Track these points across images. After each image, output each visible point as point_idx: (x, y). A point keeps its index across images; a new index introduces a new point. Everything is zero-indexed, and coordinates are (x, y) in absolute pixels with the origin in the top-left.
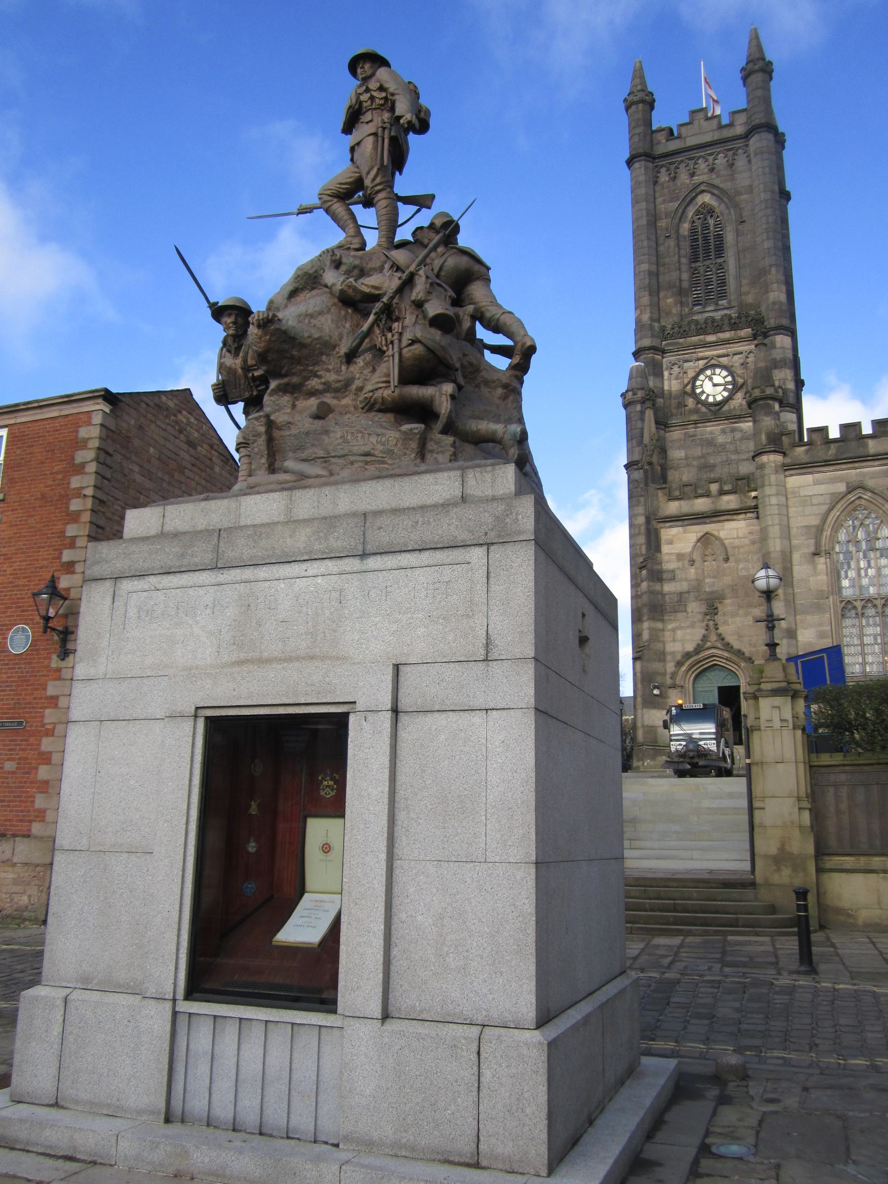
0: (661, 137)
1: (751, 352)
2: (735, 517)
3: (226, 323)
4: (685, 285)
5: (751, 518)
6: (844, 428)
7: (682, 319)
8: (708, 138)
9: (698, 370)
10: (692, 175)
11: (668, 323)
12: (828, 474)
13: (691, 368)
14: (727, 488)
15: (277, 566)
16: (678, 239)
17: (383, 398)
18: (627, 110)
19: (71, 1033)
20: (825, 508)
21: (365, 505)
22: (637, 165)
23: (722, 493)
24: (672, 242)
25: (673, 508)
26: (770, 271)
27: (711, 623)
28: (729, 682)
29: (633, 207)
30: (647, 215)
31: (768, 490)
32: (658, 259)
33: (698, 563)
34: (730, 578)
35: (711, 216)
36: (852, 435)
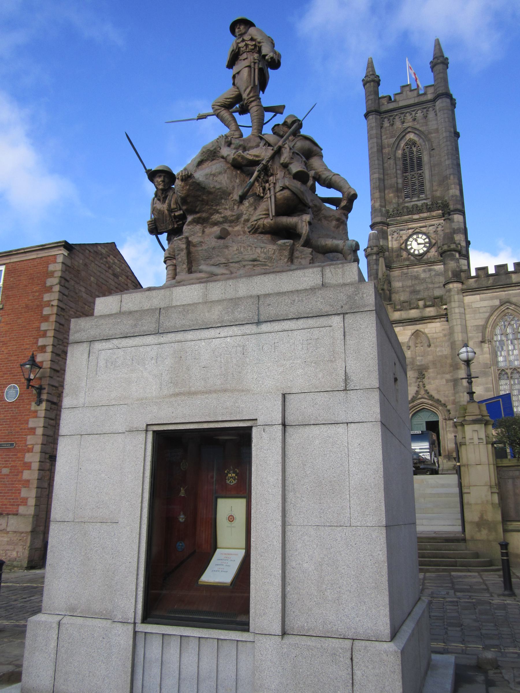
0: (384, 101)
1: (439, 224)
2: (433, 321)
3: (157, 181)
4: (400, 186)
5: (442, 321)
6: (497, 267)
7: (398, 206)
8: (411, 102)
9: (408, 235)
10: (403, 123)
11: (390, 208)
12: (489, 294)
13: (404, 234)
14: (428, 303)
15: (199, 331)
16: (395, 159)
17: (263, 224)
18: (364, 85)
19: (63, 646)
20: (488, 314)
22: (370, 117)
23: (426, 306)
24: (392, 162)
26: (450, 177)
27: (421, 383)
28: (432, 419)
29: (369, 141)
30: (377, 146)
31: (453, 305)
32: (384, 171)
33: (412, 348)
34: (432, 356)
35: (415, 146)
36: (503, 272)
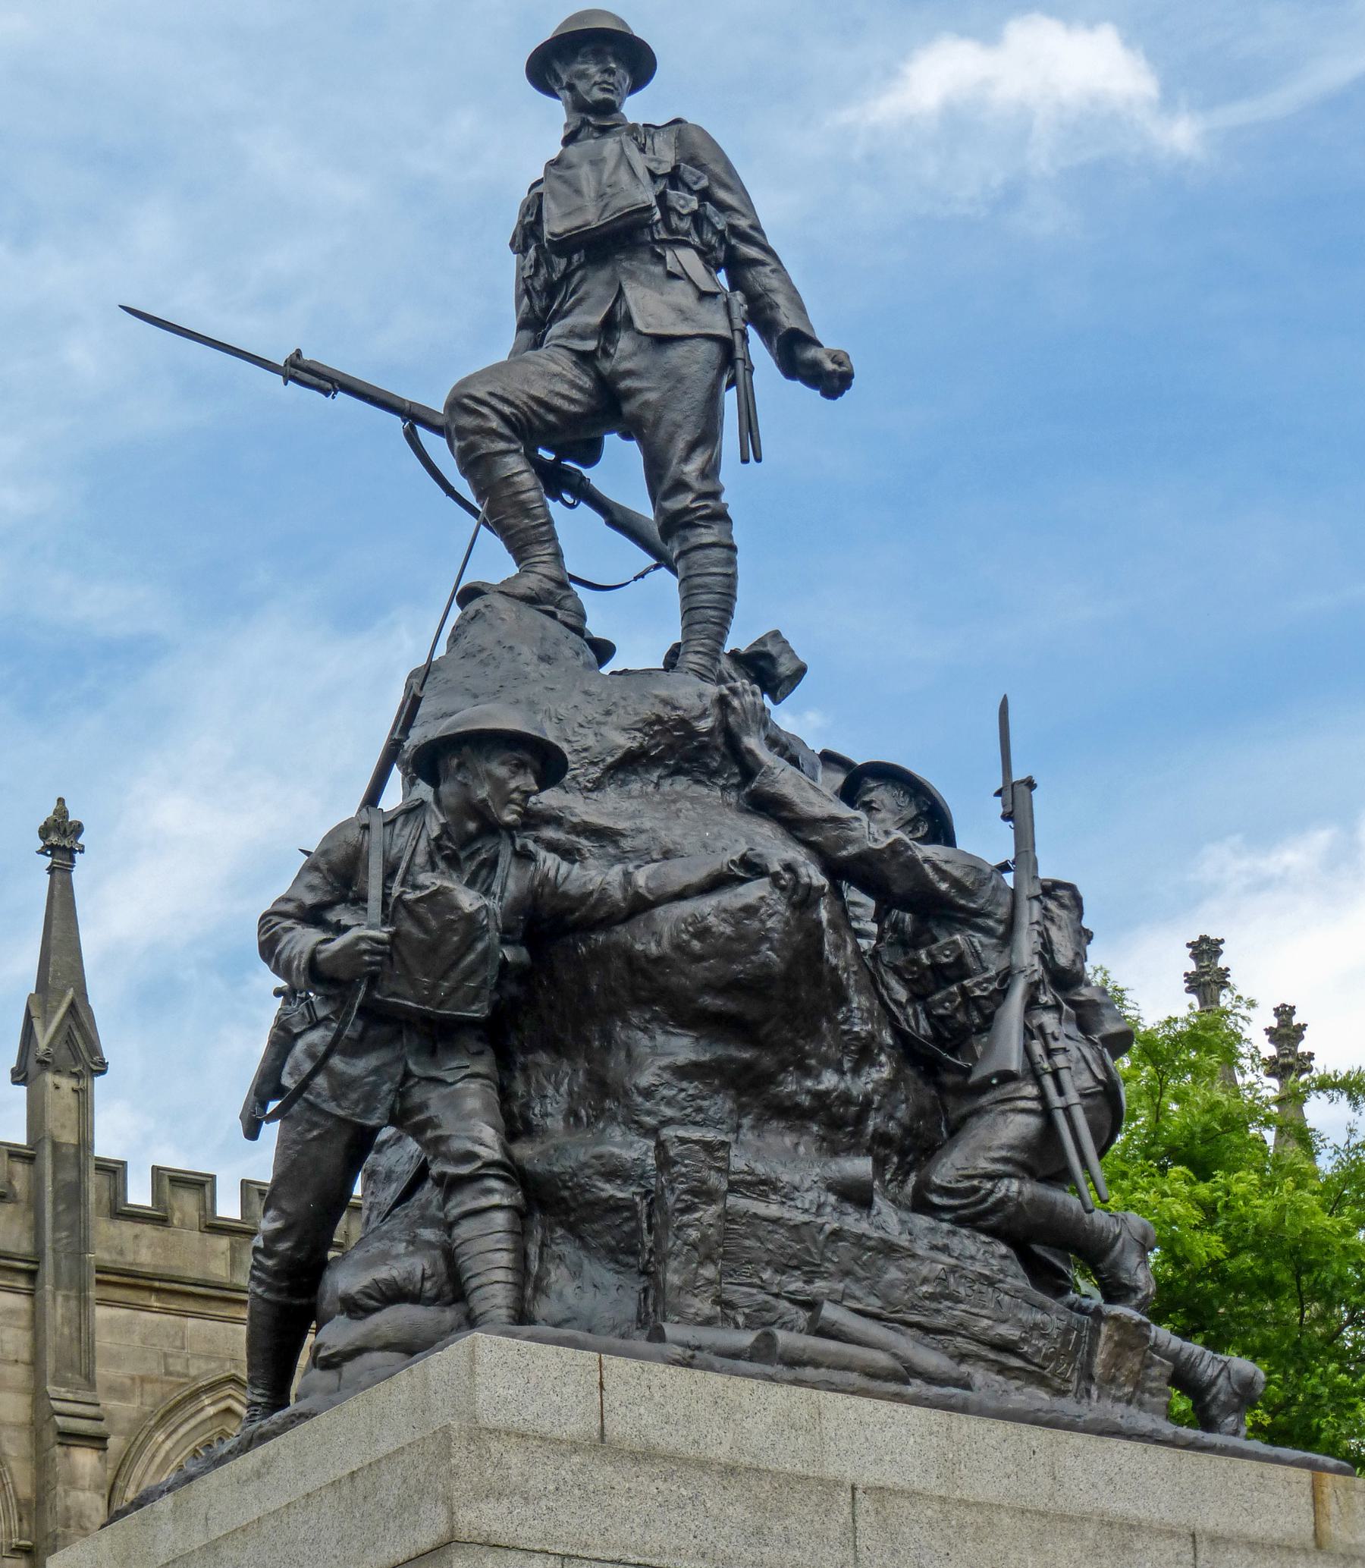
21: (1212, 1519)
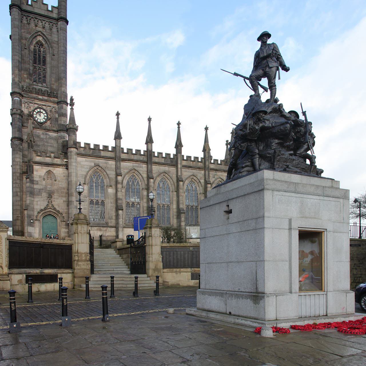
2: (59, 167)
4: (31, 72)
7: (30, 85)
8: (42, 13)
10: (36, 26)
12: (89, 159)
13: (32, 107)
20: (88, 170)
23: (55, 157)
25: (38, 159)
27: (50, 200)
31: (72, 160)
33: (46, 180)
35: (42, 47)
36: (97, 149)
